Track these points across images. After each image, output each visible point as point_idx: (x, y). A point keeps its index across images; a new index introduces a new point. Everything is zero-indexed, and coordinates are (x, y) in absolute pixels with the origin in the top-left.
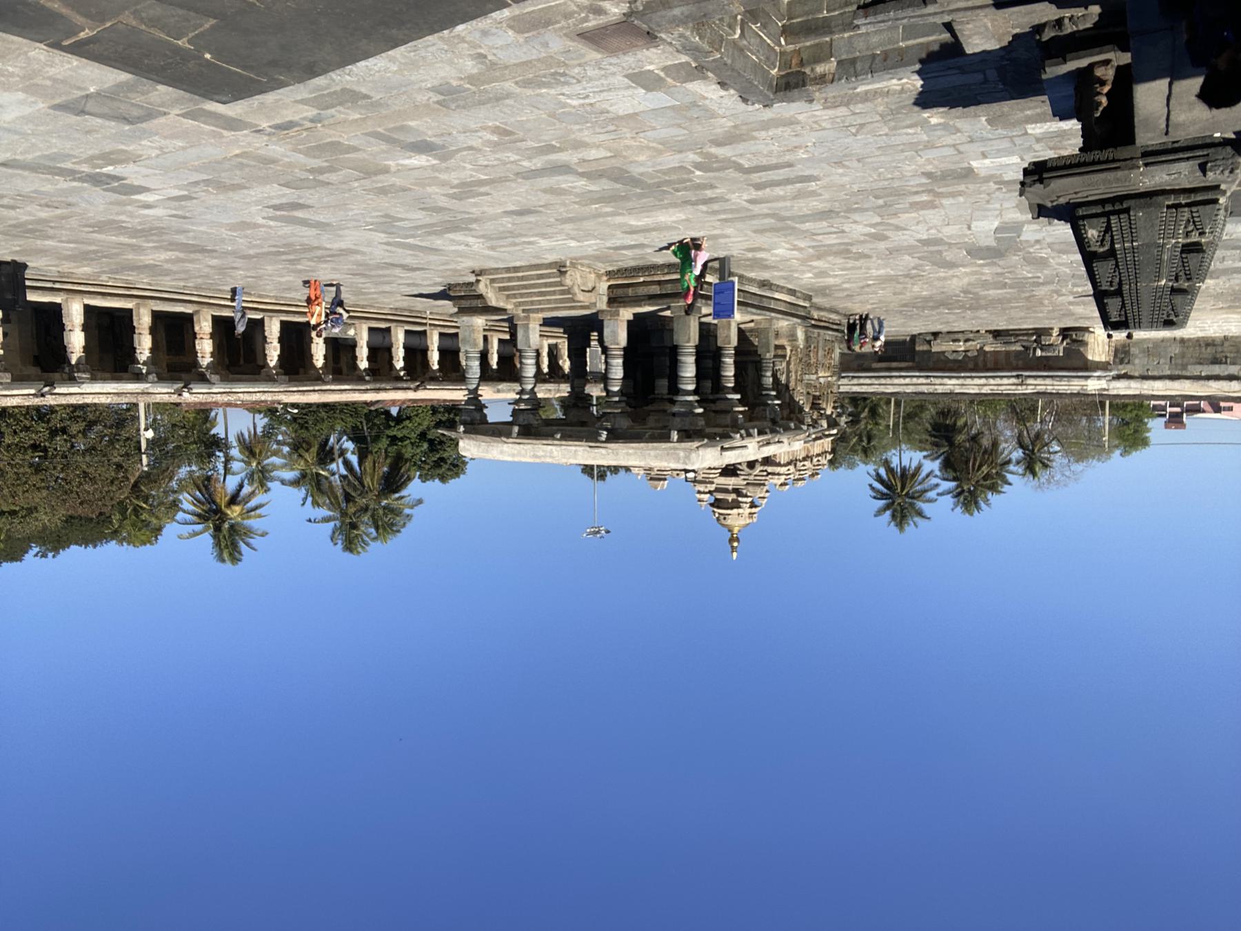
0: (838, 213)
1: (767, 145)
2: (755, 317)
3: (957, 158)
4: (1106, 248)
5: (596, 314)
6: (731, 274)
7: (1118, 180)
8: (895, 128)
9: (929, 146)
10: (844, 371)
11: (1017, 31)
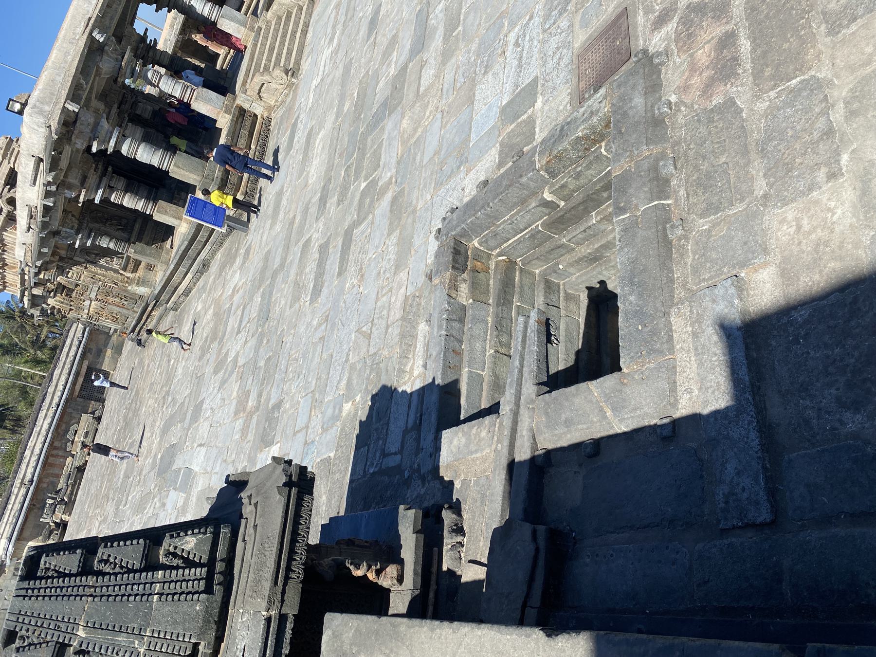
0: (263, 326)
1: (377, 247)
2: (175, 250)
3: (289, 432)
4: (162, 559)
5: (234, 93)
6: (231, 229)
7: (258, 581)
8: (352, 368)
9: (316, 403)
10: (91, 333)
11: (457, 485)
